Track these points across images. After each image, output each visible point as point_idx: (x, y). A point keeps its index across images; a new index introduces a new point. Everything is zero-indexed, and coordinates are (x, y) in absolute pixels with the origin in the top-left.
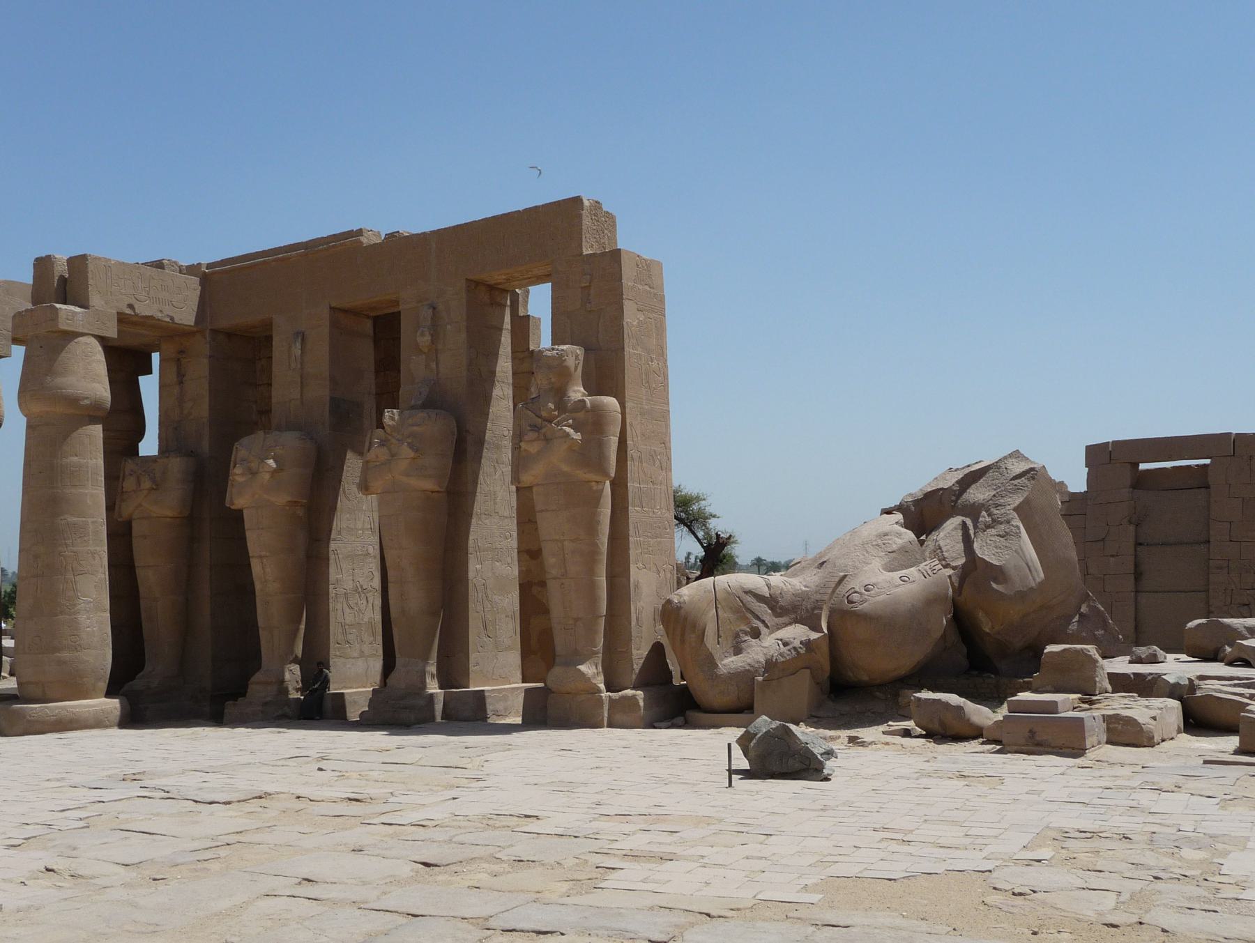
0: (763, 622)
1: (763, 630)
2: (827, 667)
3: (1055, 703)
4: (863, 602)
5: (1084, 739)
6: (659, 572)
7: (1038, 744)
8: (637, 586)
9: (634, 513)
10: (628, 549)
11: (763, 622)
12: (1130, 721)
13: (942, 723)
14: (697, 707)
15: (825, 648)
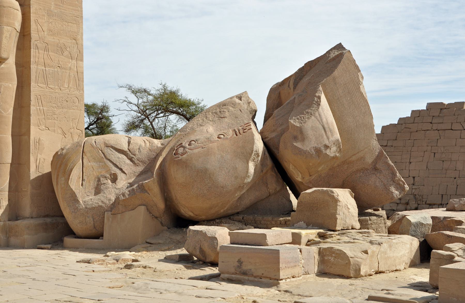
0: (121, 169)
1: (120, 176)
2: (161, 205)
3: (264, 235)
4: (183, 154)
5: (278, 270)
6: (64, 134)
7: (245, 273)
8: (39, 142)
9: (35, 89)
10: (29, 115)
11: (121, 169)
12: (341, 255)
13: (202, 251)
14: (71, 233)
15: (156, 190)
